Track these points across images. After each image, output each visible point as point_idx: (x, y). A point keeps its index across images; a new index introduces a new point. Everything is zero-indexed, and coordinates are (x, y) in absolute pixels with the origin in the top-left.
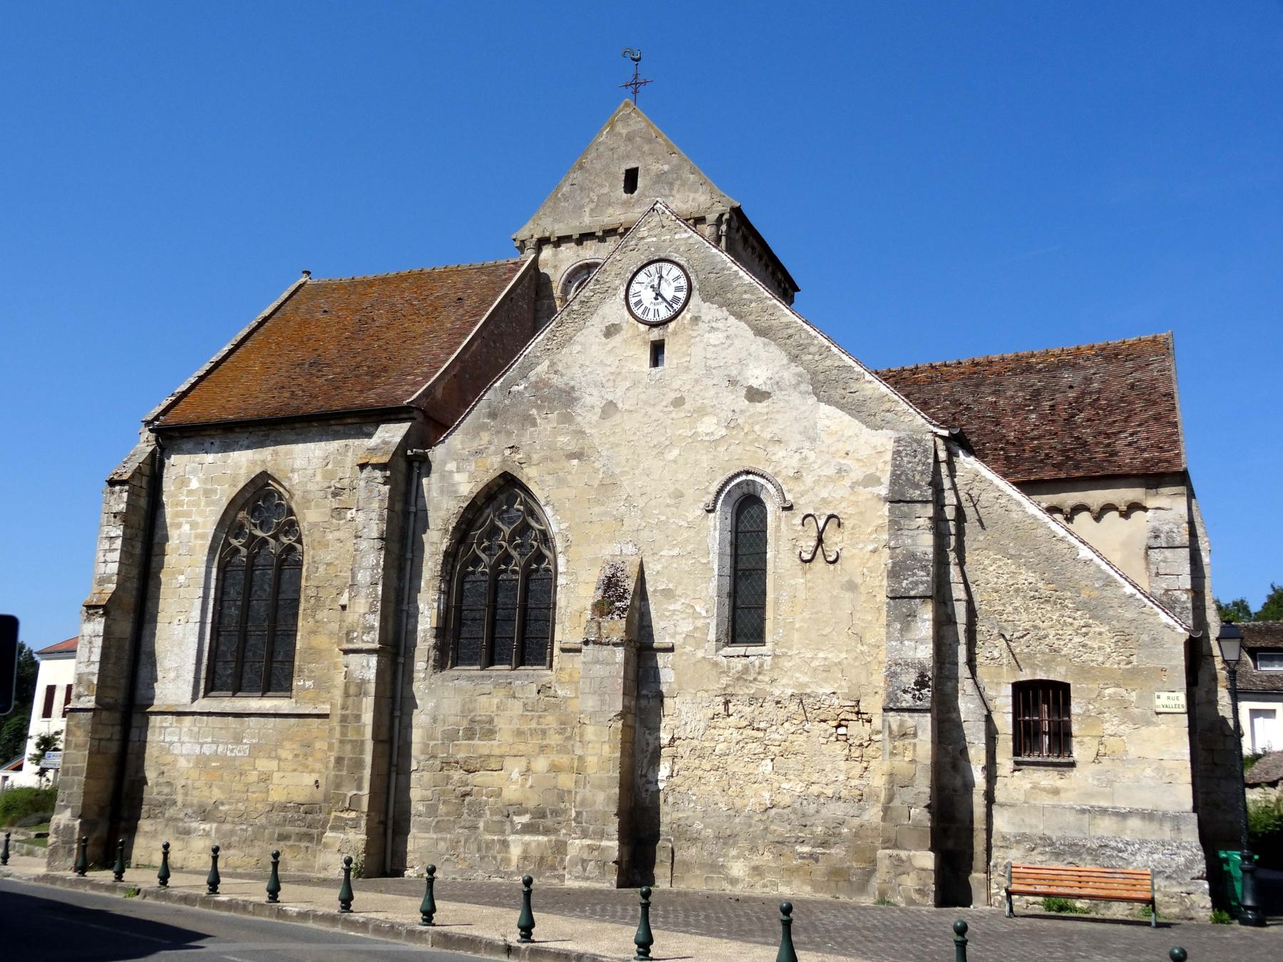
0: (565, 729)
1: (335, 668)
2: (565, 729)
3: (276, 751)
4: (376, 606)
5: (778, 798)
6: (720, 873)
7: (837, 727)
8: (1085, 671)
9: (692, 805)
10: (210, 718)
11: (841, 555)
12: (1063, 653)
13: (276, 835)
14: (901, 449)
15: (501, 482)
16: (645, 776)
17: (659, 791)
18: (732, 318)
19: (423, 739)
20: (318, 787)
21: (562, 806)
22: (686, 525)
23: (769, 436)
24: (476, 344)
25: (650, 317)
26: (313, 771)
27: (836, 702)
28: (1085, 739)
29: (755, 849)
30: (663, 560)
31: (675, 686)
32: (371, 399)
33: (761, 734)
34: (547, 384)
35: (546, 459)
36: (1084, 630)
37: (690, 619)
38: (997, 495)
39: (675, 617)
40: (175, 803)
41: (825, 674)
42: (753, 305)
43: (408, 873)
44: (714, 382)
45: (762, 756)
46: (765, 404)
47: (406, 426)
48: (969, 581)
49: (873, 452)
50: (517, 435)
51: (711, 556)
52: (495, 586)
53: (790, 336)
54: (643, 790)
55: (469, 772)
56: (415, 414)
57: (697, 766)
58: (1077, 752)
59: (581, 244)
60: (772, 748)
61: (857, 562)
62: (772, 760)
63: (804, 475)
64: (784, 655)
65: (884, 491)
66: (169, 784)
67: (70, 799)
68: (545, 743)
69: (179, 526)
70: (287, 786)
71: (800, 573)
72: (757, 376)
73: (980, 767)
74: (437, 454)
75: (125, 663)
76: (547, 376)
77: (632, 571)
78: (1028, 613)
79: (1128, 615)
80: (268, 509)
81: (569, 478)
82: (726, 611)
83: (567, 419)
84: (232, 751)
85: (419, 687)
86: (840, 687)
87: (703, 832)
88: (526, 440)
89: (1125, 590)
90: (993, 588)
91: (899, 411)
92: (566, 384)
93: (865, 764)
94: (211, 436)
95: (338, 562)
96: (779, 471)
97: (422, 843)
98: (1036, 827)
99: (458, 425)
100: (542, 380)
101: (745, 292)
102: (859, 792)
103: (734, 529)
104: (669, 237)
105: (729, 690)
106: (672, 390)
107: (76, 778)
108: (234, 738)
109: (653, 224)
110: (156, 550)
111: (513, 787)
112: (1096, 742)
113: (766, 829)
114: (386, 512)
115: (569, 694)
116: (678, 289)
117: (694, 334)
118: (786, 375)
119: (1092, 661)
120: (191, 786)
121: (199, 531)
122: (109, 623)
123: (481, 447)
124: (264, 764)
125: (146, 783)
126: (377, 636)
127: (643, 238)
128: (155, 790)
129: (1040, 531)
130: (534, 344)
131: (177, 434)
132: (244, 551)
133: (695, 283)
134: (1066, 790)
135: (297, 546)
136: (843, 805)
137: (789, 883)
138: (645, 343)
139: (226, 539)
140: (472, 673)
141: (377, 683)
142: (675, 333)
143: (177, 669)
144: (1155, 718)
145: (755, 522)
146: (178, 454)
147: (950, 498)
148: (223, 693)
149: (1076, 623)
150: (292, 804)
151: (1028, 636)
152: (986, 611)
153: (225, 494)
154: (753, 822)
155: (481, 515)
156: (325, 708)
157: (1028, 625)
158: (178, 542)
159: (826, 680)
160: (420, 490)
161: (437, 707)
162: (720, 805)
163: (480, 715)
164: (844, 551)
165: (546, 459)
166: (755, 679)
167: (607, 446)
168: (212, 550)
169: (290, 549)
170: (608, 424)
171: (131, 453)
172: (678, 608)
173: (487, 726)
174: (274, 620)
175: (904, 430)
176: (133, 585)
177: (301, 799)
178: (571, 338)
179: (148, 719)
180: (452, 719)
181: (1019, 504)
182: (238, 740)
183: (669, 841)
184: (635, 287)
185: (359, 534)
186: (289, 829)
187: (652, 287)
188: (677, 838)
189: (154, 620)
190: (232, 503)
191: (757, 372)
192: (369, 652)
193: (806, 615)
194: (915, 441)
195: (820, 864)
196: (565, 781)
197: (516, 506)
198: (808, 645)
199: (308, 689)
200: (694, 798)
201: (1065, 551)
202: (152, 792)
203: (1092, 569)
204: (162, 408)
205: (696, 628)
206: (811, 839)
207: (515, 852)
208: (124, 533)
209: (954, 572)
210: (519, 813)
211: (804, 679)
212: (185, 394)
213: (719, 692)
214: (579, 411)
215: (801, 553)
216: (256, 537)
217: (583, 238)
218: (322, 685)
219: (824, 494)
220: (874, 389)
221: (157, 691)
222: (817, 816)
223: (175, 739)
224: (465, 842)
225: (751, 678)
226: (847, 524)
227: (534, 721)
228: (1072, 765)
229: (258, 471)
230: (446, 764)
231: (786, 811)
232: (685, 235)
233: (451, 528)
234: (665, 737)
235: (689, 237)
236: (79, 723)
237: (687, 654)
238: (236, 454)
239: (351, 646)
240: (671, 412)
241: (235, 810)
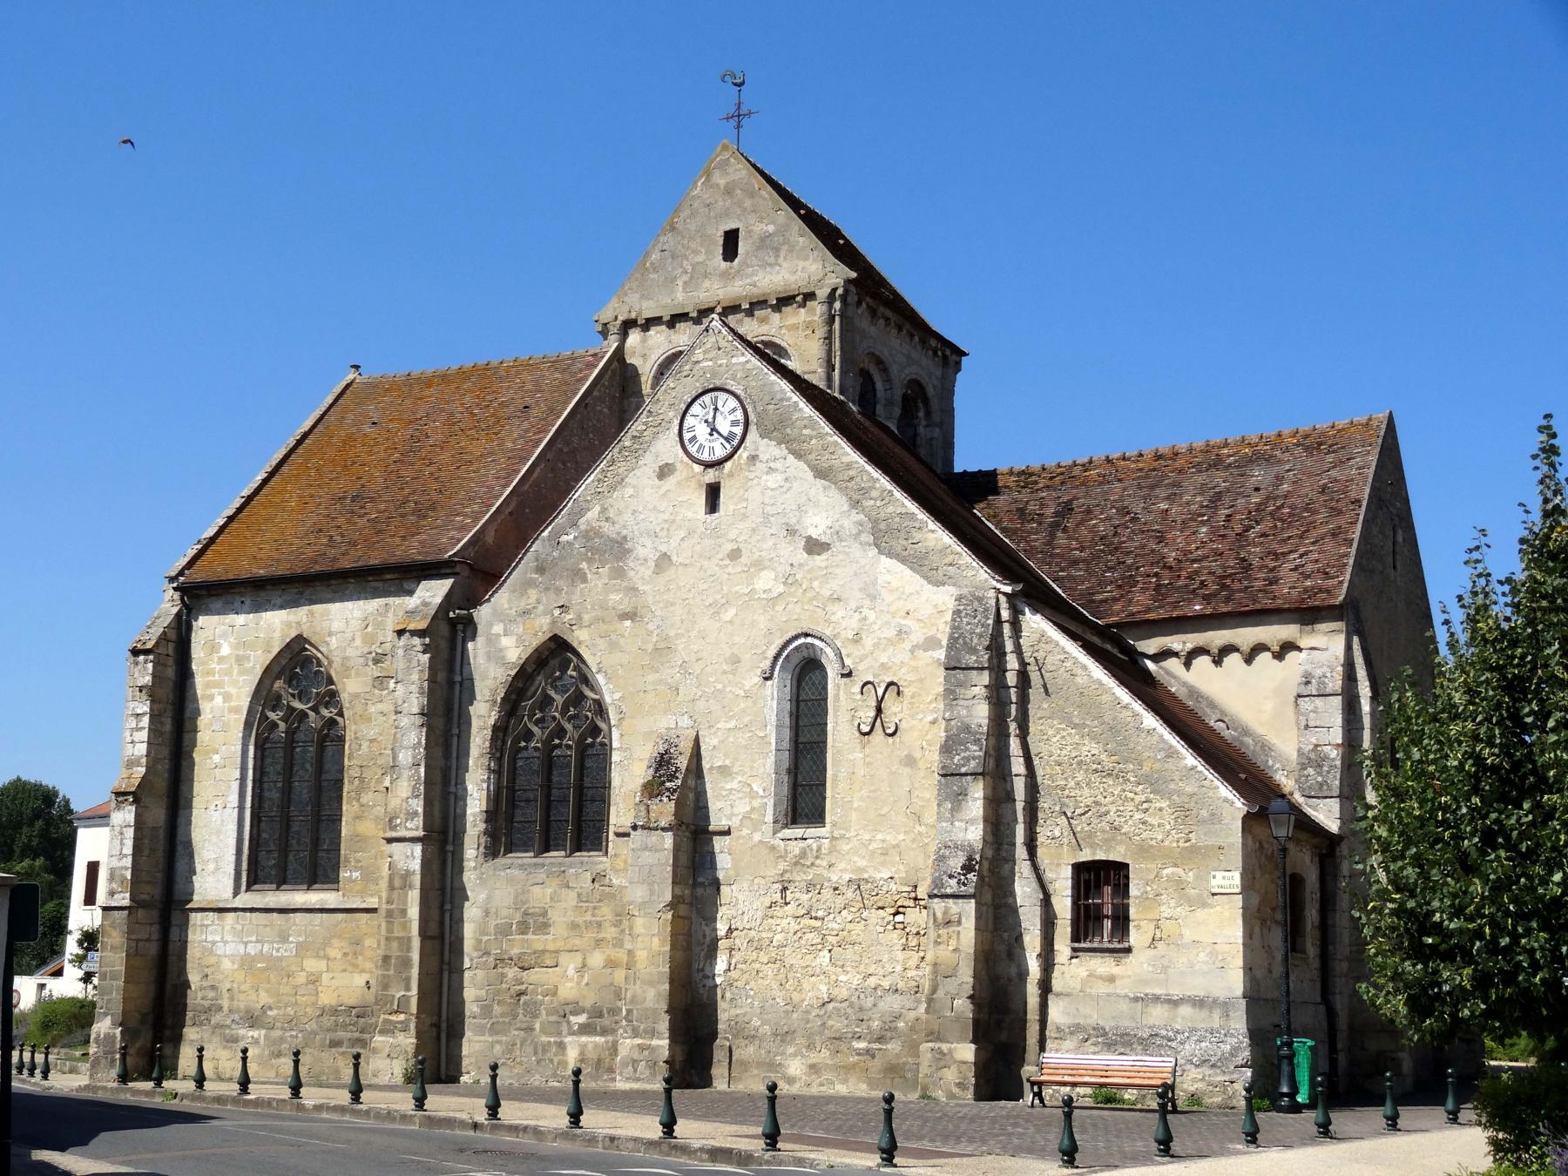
0: (620, 920)
1: (382, 858)
2: (620, 920)
3: (324, 949)
4: (419, 789)
5: (835, 992)
6: (777, 1072)
8: (1144, 850)
9: (750, 1000)
10: (254, 914)
11: (900, 726)
12: (1123, 831)
13: (328, 1042)
14: (962, 608)
15: (553, 645)
16: (703, 970)
17: (716, 986)
18: (791, 458)
19: (475, 932)
20: (369, 988)
24: (538, 470)
25: (705, 456)
26: (363, 971)
27: (893, 887)
28: (1142, 923)
29: (812, 1046)
30: (719, 734)
31: (732, 872)
32: (412, 550)
33: (818, 924)
34: (598, 534)
35: (598, 619)
36: (1145, 805)
38: (1062, 657)
39: (731, 797)
40: (220, 1008)
41: (883, 857)
42: (814, 441)
43: (464, 1079)
44: (772, 531)
45: (819, 947)
46: (824, 556)
47: (448, 582)
48: (1033, 752)
49: (934, 611)
50: (567, 593)
51: (768, 728)
52: (549, 763)
53: (852, 478)
55: (523, 969)
56: (458, 569)
57: (754, 958)
58: (1135, 938)
59: (674, 327)
60: (830, 938)
61: (916, 734)
62: (830, 951)
63: (864, 637)
64: (843, 837)
65: (941, 654)
66: (213, 987)
67: (109, 1006)
68: (600, 936)
69: (211, 698)
70: (338, 988)
71: (859, 747)
72: (816, 525)
73: (1035, 955)
74: (482, 614)
75: (160, 854)
77: (686, 746)
78: (1090, 788)
79: (1189, 789)
80: (306, 677)
81: (622, 641)
82: (785, 790)
83: (619, 573)
84: (278, 951)
85: (469, 877)
87: (761, 1030)
88: (576, 599)
89: (1187, 762)
90: (1056, 761)
91: (961, 565)
92: (619, 533)
93: (922, 954)
94: (241, 594)
95: (381, 738)
96: (839, 633)
97: (477, 1047)
98: (1091, 1017)
99: (504, 581)
100: (593, 529)
101: (805, 426)
102: (916, 984)
103: (795, 698)
104: (725, 361)
107: (114, 983)
108: (280, 936)
109: (708, 345)
110: (187, 725)
111: (569, 985)
112: (1152, 926)
114: (426, 683)
115: (624, 882)
117: (751, 476)
119: (1152, 839)
120: (236, 990)
121: (232, 704)
122: (139, 811)
124: (312, 965)
125: (190, 987)
126: (421, 823)
127: (698, 362)
128: (200, 995)
129: (1105, 698)
130: (584, 486)
131: (204, 592)
132: (282, 726)
133: (752, 417)
134: (1122, 977)
135: (339, 719)
137: (845, 1081)
138: (701, 486)
139: (263, 713)
140: (525, 861)
141: (423, 875)
142: (731, 475)
143: (216, 860)
144: (1211, 900)
145: (817, 689)
146: (207, 615)
147: (1012, 663)
148: (266, 887)
149: (1138, 799)
150: (343, 1008)
151: (1090, 813)
152: (1049, 786)
153: (259, 660)
154: (811, 1017)
155: (532, 684)
156: (372, 902)
157: (1089, 801)
158: (210, 716)
159: (883, 864)
160: (465, 657)
161: (489, 898)
162: (778, 1000)
163: (534, 907)
165: (598, 619)
167: (661, 605)
168: (248, 725)
169: (332, 723)
170: (662, 579)
171: (156, 615)
172: (735, 787)
173: (541, 919)
174: (317, 804)
176: (164, 767)
177: (352, 1002)
178: (623, 480)
179: (188, 916)
180: (504, 912)
181: (1085, 668)
182: (284, 938)
183: (727, 1039)
184: (689, 421)
185: (399, 709)
186: (341, 1034)
187: (706, 421)
188: (735, 1036)
189: (189, 806)
190: (267, 671)
191: (816, 520)
192: (413, 840)
193: (864, 793)
196: (619, 975)
197: (569, 672)
198: (867, 825)
199: (356, 880)
200: (752, 993)
201: (1129, 719)
202: (196, 996)
203: (1156, 738)
204: (187, 559)
205: (753, 809)
208: (151, 709)
209: (1014, 745)
210: (575, 1013)
211: (862, 863)
212: (212, 540)
214: (631, 564)
216: (294, 709)
217: (675, 320)
218: (369, 876)
219: (884, 659)
220: (937, 539)
221: (197, 885)
222: (875, 1010)
223: (218, 938)
224: (521, 1045)
225: (809, 863)
226: (906, 691)
227: (589, 913)
228: (1128, 950)
229: (293, 635)
230: (500, 961)
231: (843, 1005)
232: (743, 359)
233: (499, 700)
234: (722, 928)
235: (747, 362)
236: (114, 922)
237: (744, 837)
238: (269, 614)
239: (394, 834)
240: (727, 566)
241: (284, 1015)
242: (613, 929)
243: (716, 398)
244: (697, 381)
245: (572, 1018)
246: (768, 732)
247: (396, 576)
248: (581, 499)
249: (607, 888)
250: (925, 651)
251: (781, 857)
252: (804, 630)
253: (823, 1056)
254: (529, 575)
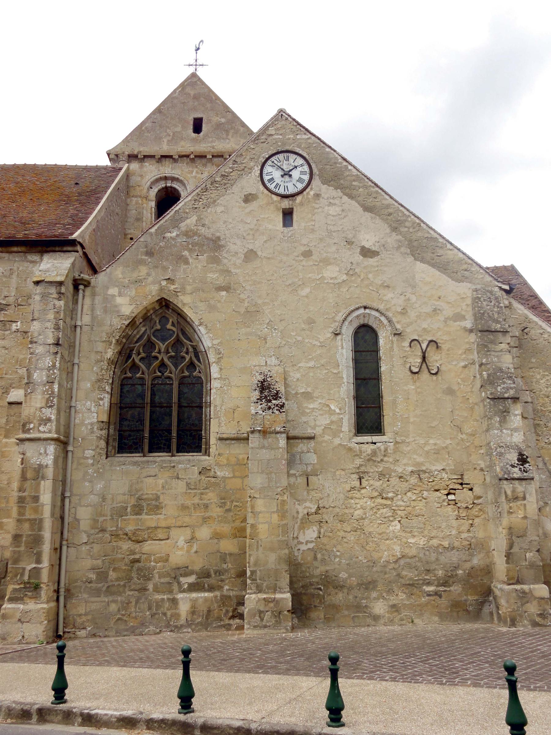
5: (407, 551)
6: (365, 612)
7: (447, 495)
9: (337, 560)
14: (480, 296)
16: (297, 538)
18: (345, 198)
21: (225, 566)
22: (319, 344)
23: (380, 283)
25: (281, 191)
27: (445, 476)
29: (391, 591)
30: (301, 370)
31: (317, 467)
33: (389, 502)
35: (197, 290)
39: (314, 414)
41: (435, 456)
42: (361, 190)
44: (335, 241)
46: (376, 259)
50: (172, 270)
51: (340, 367)
53: (390, 214)
54: (296, 550)
55: (139, 542)
62: (399, 521)
63: (409, 311)
64: (403, 442)
68: (207, 514)
76: (195, 227)
81: (219, 305)
83: (215, 260)
86: (448, 465)
88: (180, 275)
91: (473, 271)
93: (471, 522)
96: (390, 308)
100: (191, 230)
101: (354, 181)
102: (468, 543)
105: (363, 469)
106: (301, 245)
111: (180, 553)
113: (398, 575)
116: (302, 173)
117: (317, 206)
118: (389, 240)
123: (141, 278)
133: (315, 170)
136: (457, 553)
140: (137, 459)
142: (301, 204)
154: (388, 570)
162: (360, 558)
163: (147, 494)
164: (443, 366)
165: (197, 290)
166: (382, 460)
175: (478, 284)
178: (215, 201)
180: (120, 498)
183: (320, 589)
184: (268, 169)
191: (367, 237)
194: (488, 291)
195: (443, 599)
200: (338, 554)
205: (332, 422)
206: (434, 580)
207: (184, 608)
210: (186, 575)
211: (420, 459)
213: (354, 471)
215: (410, 367)
219: (425, 325)
225: (379, 460)
226: (444, 347)
230: (115, 535)
231: (413, 560)
235: (309, 138)
237: (326, 442)
240: (301, 261)
242: (218, 509)
243: (288, 157)
244: (271, 146)
245: (182, 579)
246: (340, 370)
247: (23, 249)
248: (181, 211)
249: (213, 479)
250: (455, 321)
251: (357, 455)
252: (364, 304)
253: (401, 597)
254: (139, 257)
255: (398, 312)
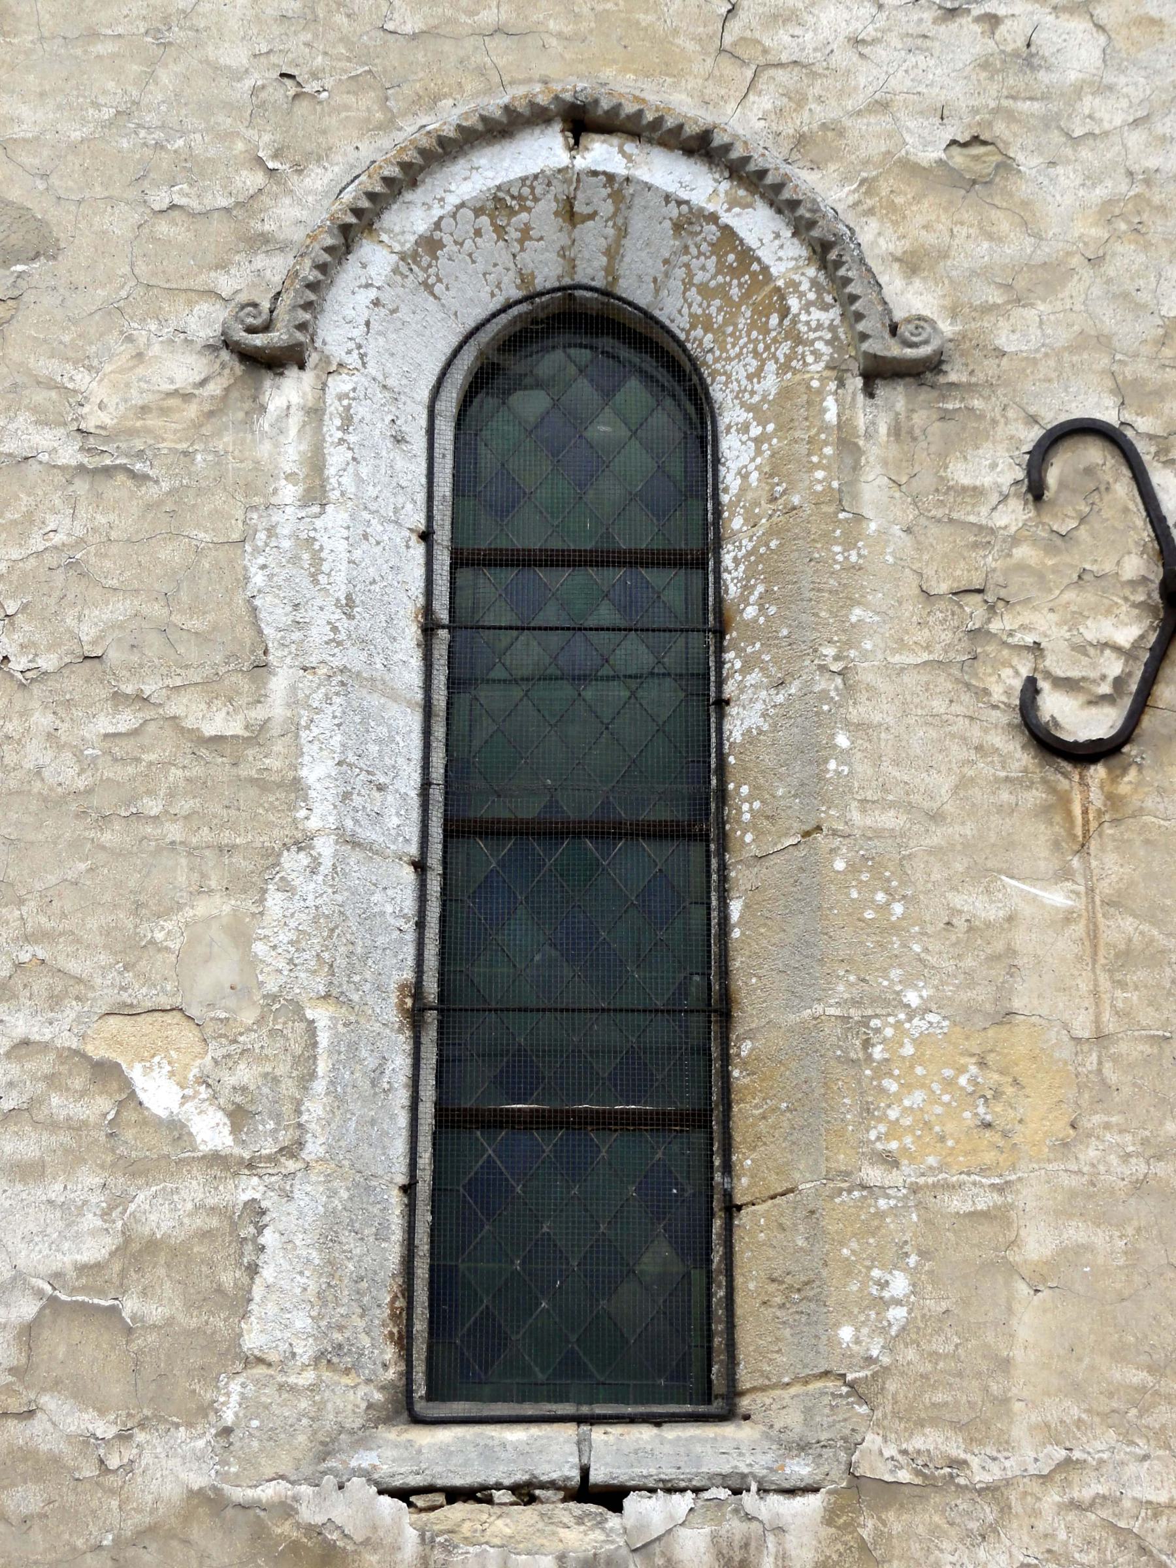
22: (70, 454)
37: (88, 1178)
51: (278, 685)
63: (1028, 162)
96: (835, 129)
215: (1031, 689)
246: (276, 707)
255: (910, 168)
